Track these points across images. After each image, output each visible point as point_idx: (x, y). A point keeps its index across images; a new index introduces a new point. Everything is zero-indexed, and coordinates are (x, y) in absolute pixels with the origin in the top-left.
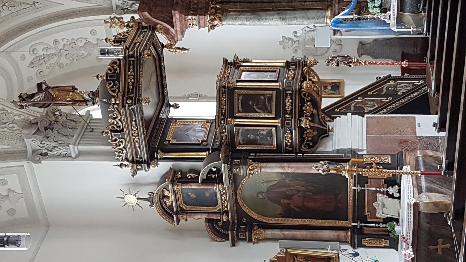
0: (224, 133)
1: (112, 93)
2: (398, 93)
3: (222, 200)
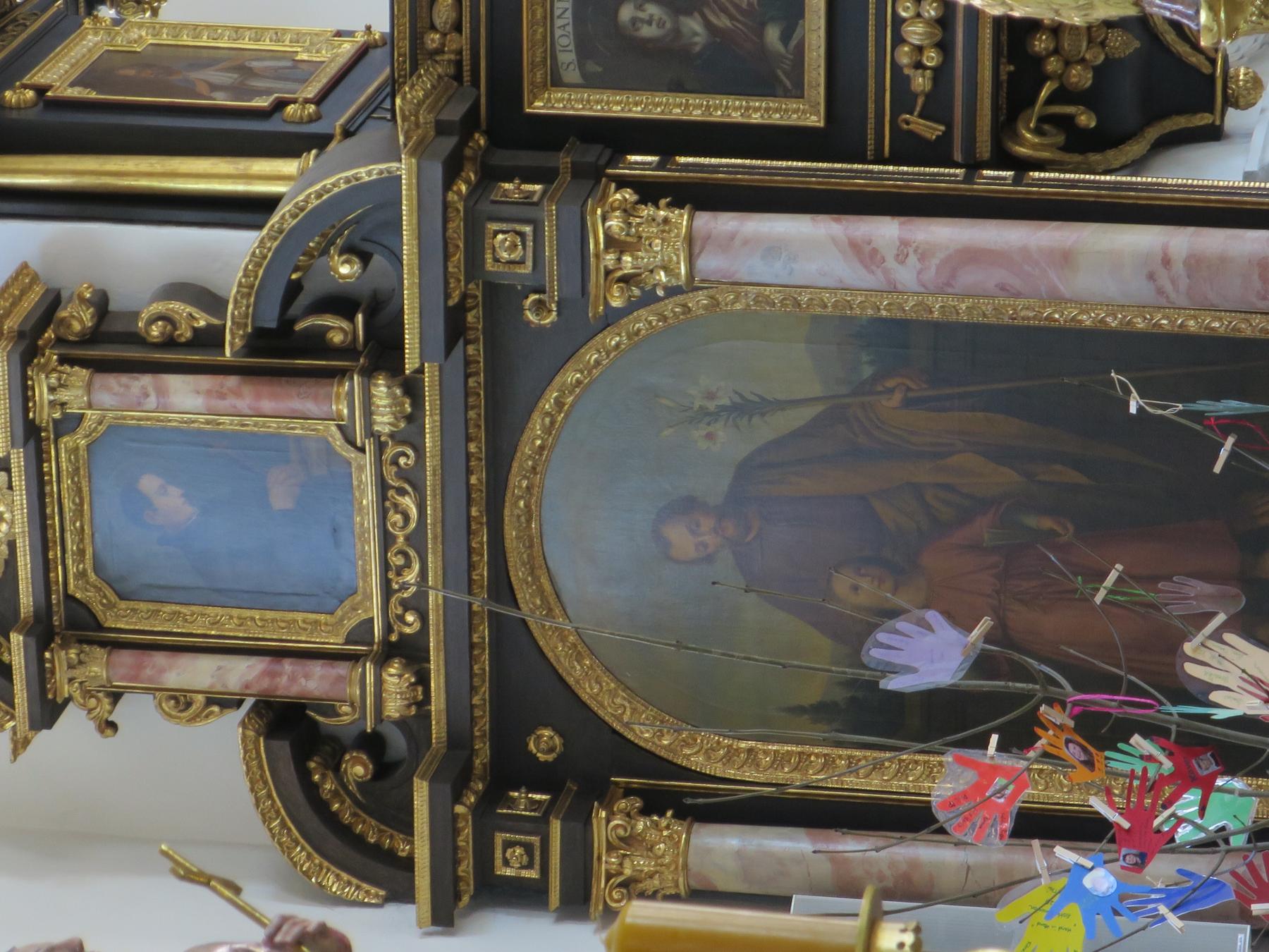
3: (387, 540)
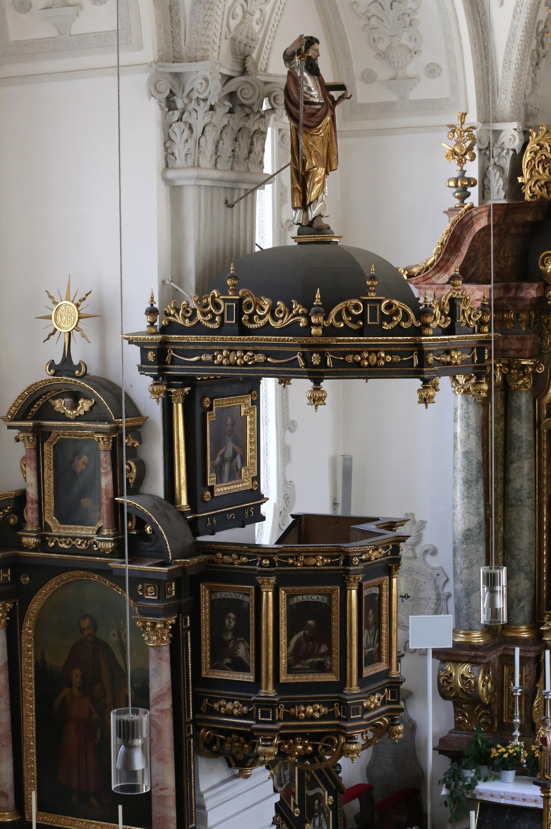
0: (239, 559)
1: (335, 314)
2: (308, 825)
3: (74, 538)
